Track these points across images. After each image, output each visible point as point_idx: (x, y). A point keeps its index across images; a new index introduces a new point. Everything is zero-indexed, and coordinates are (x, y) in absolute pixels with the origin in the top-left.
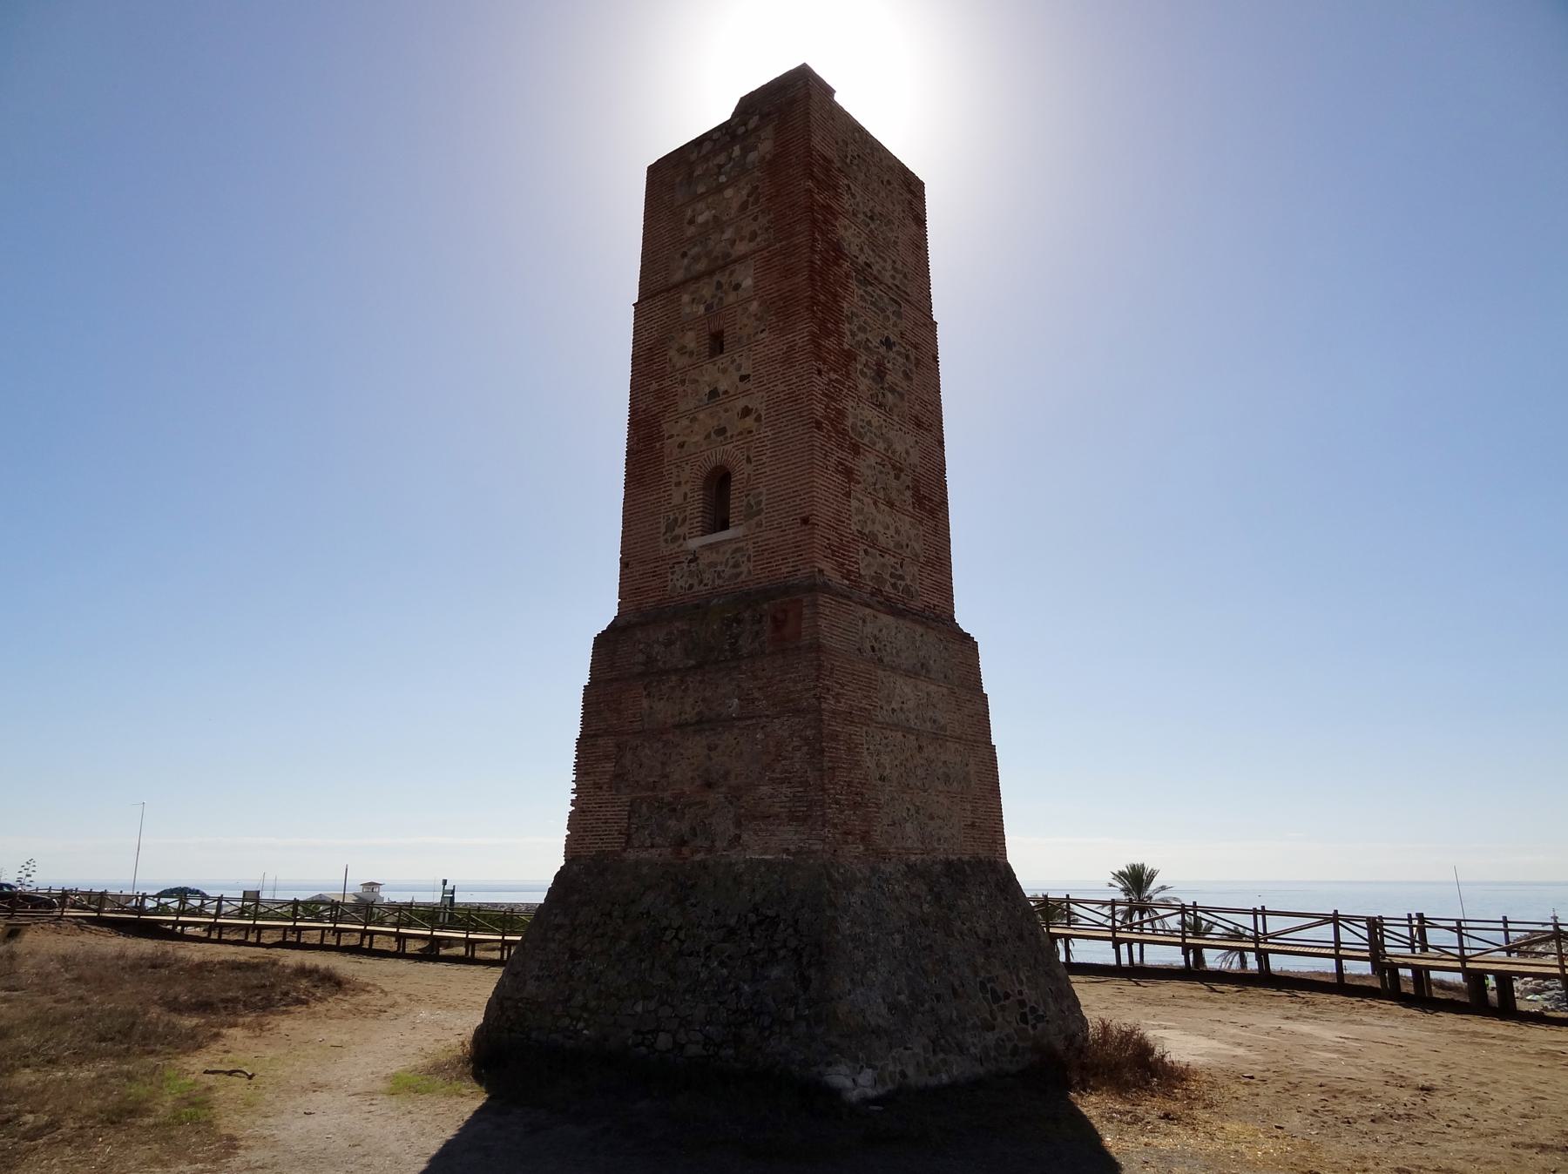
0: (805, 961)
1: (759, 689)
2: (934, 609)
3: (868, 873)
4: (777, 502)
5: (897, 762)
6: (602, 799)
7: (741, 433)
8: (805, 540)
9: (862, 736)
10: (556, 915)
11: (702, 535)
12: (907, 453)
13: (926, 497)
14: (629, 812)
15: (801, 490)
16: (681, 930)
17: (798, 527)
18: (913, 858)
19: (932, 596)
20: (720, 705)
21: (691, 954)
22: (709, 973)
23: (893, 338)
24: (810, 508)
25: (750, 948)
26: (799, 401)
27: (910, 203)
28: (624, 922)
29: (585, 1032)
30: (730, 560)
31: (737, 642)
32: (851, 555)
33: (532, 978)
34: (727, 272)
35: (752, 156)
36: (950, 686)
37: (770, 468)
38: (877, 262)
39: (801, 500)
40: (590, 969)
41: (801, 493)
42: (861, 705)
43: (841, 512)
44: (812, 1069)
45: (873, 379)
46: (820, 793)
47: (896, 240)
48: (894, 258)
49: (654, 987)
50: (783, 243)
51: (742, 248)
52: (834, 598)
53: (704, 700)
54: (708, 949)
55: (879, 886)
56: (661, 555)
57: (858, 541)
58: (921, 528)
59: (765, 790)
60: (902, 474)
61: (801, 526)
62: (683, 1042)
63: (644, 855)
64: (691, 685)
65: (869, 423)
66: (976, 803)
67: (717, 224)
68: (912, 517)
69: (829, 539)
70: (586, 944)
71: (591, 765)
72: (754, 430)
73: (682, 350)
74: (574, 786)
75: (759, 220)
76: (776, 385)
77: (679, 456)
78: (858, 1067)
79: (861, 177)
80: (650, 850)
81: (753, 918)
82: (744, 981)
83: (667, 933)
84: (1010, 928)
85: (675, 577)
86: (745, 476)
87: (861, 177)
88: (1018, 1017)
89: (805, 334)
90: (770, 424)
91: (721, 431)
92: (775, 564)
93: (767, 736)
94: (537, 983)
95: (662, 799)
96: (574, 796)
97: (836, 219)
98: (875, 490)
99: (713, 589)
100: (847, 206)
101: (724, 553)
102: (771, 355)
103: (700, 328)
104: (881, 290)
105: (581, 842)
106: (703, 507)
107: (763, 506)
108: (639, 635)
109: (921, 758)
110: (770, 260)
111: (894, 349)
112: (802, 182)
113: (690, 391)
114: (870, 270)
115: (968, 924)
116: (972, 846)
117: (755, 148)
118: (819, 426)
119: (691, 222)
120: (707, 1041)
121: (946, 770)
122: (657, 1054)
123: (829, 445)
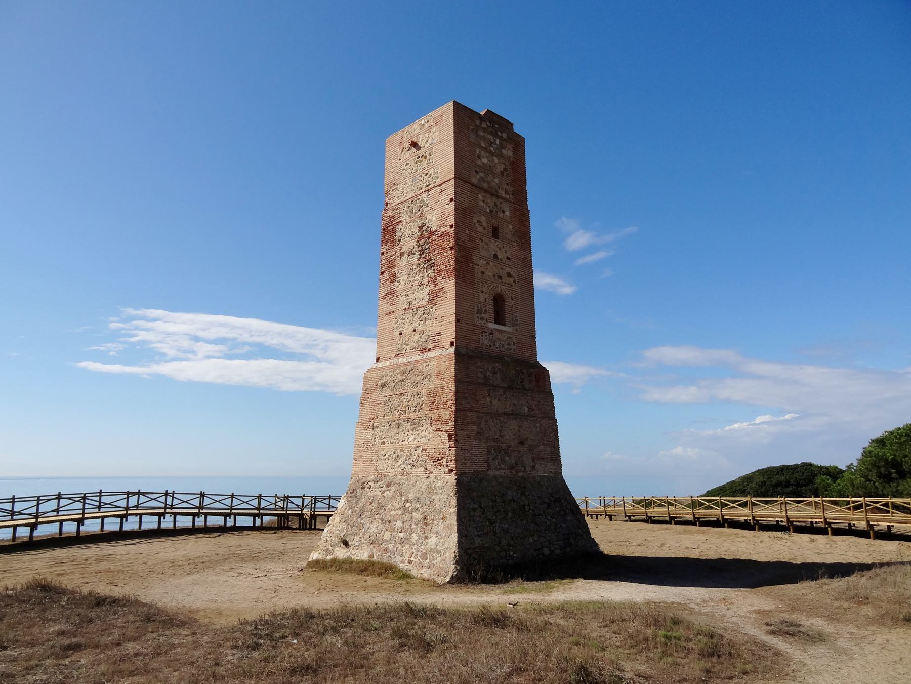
1: (536, 405)
7: (508, 284)
21: (539, 515)
29: (515, 555)
31: (523, 382)
33: (476, 536)
53: (514, 404)
59: (542, 448)
62: (553, 550)
63: (497, 473)
64: (508, 396)
71: (465, 425)
80: (500, 471)
93: (540, 425)
94: (480, 538)
95: (501, 447)
101: (504, 336)
108: (479, 364)
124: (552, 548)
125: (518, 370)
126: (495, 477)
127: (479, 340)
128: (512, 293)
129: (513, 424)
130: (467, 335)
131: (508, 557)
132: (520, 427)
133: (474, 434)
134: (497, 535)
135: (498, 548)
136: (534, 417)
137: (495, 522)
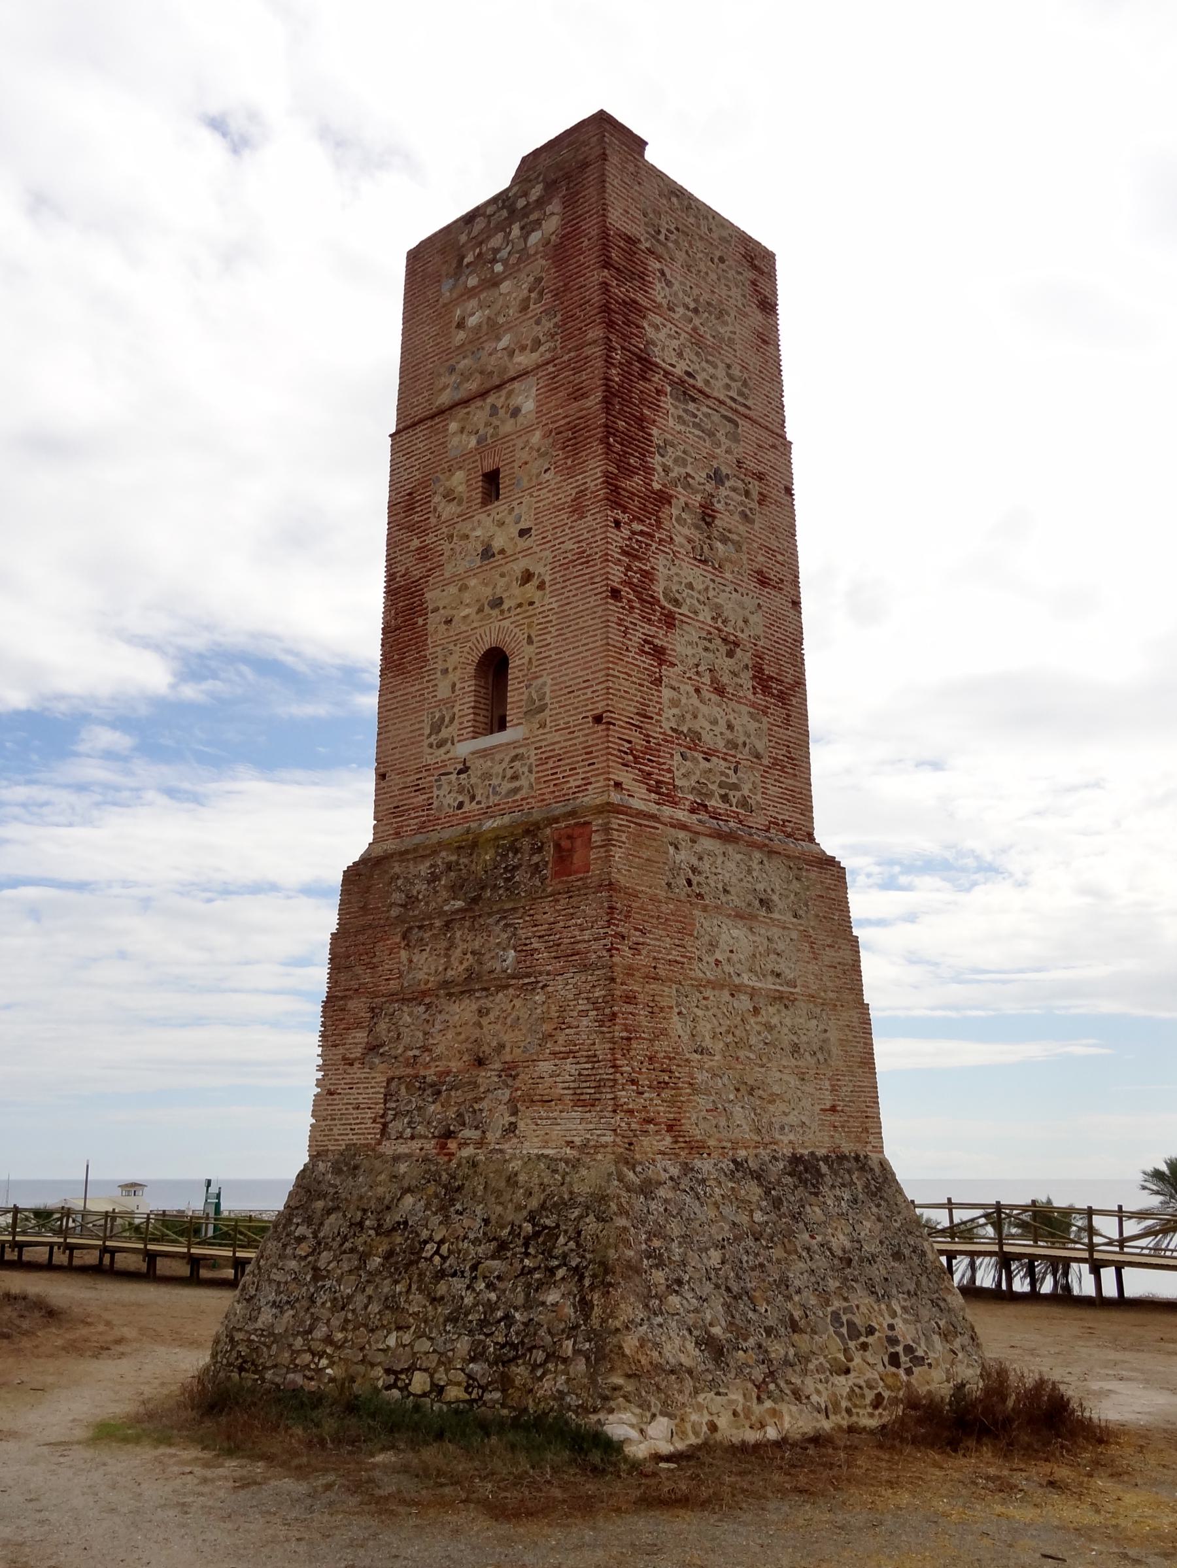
0: (587, 1283)
2: (783, 826)
3: (675, 1171)
4: (565, 695)
5: (723, 1029)
6: (353, 1078)
7: (520, 605)
8: (597, 745)
9: (671, 997)
10: (298, 1225)
11: (474, 738)
12: (746, 621)
13: (772, 678)
14: (385, 1095)
15: (594, 679)
16: (444, 1244)
17: (589, 728)
18: (742, 1153)
19: (781, 808)
20: (493, 958)
21: (454, 1275)
22: (475, 1298)
23: (725, 470)
24: (604, 703)
25: (524, 1267)
26: (591, 563)
27: (754, 283)
28: (377, 1234)
29: (329, 1371)
32: (662, 760)
33: (267, 1304)
34: (504, 392)
35: (535, 238)
36: (802, 928)
38: (704, 370)
39: (593, 692)
40: (335, 1292)
41: (594, 683)
42: (670, 957)
43: (648, 706)
44: (591, 1416)
45: (697, 527)
46: (611, 1070)
47: (733, 336)
48: (728, 361)
49: (411, 1315)
50: (572, 354)
51: (524, 360)
52: (634, 820)
54: (474, 1268)
55: (692, 1188)
57: (672, 742)
58: (765, 719)
60: (738, 650)
61: (593, 727)
62: (442, 1383)
63: (403, 1149)
65: (690, 586)
66: (839, 1080)
67: (493, 328)
68: (754, 707)
69: (630, 742)
70: (331, 1262)
73: (449, 496)
74: (321, 1062)
75: (543, 321)
76: (563, 542)
78: (648, 1415)
79: (680, 256)
81: (528, 1228)
82: (516, 1309)
83: (428, 1246)
84: (881, 1242)
85: (441, 793)
86: (526, 660)
87: (680, 256)
88: (886, 1359)
89: (599, 475)
90: (556, 593)
91: (497, 603)
92: (561, 776)
95: (425, 1077)
96: (320, 1075)
97: (644, 317)
98: (697, 673)
99: (488, 807)
100: (659, 299)
102: (557, 503)
103: (470, 467)
104: (708, 406)
105: (327, 1133)
106: (475, 701)
107: (547, 700)
109: (757, 1023)
110: (554, 378)
111: (727, 484)
112: (595, 272)
114: (691, 381)
115: (819, 1238)
116: (832, 1137)
117: (538, 223)
118: (615, 594)
119: (461, 325)
120: (471, 1382)
121: (795, 1038)
122: (411, 1397)
123: (629, 619)
124: (441, 1377)
126: (397, 1158)
127: (431, 801)
129: (462, 1011)
131: (310, 1370)
132: (481, 1012)
133: (357, 1052)
134: (312, 1310)
135: (299, 1342)
136: (528, 975)
137: (324, 1278)
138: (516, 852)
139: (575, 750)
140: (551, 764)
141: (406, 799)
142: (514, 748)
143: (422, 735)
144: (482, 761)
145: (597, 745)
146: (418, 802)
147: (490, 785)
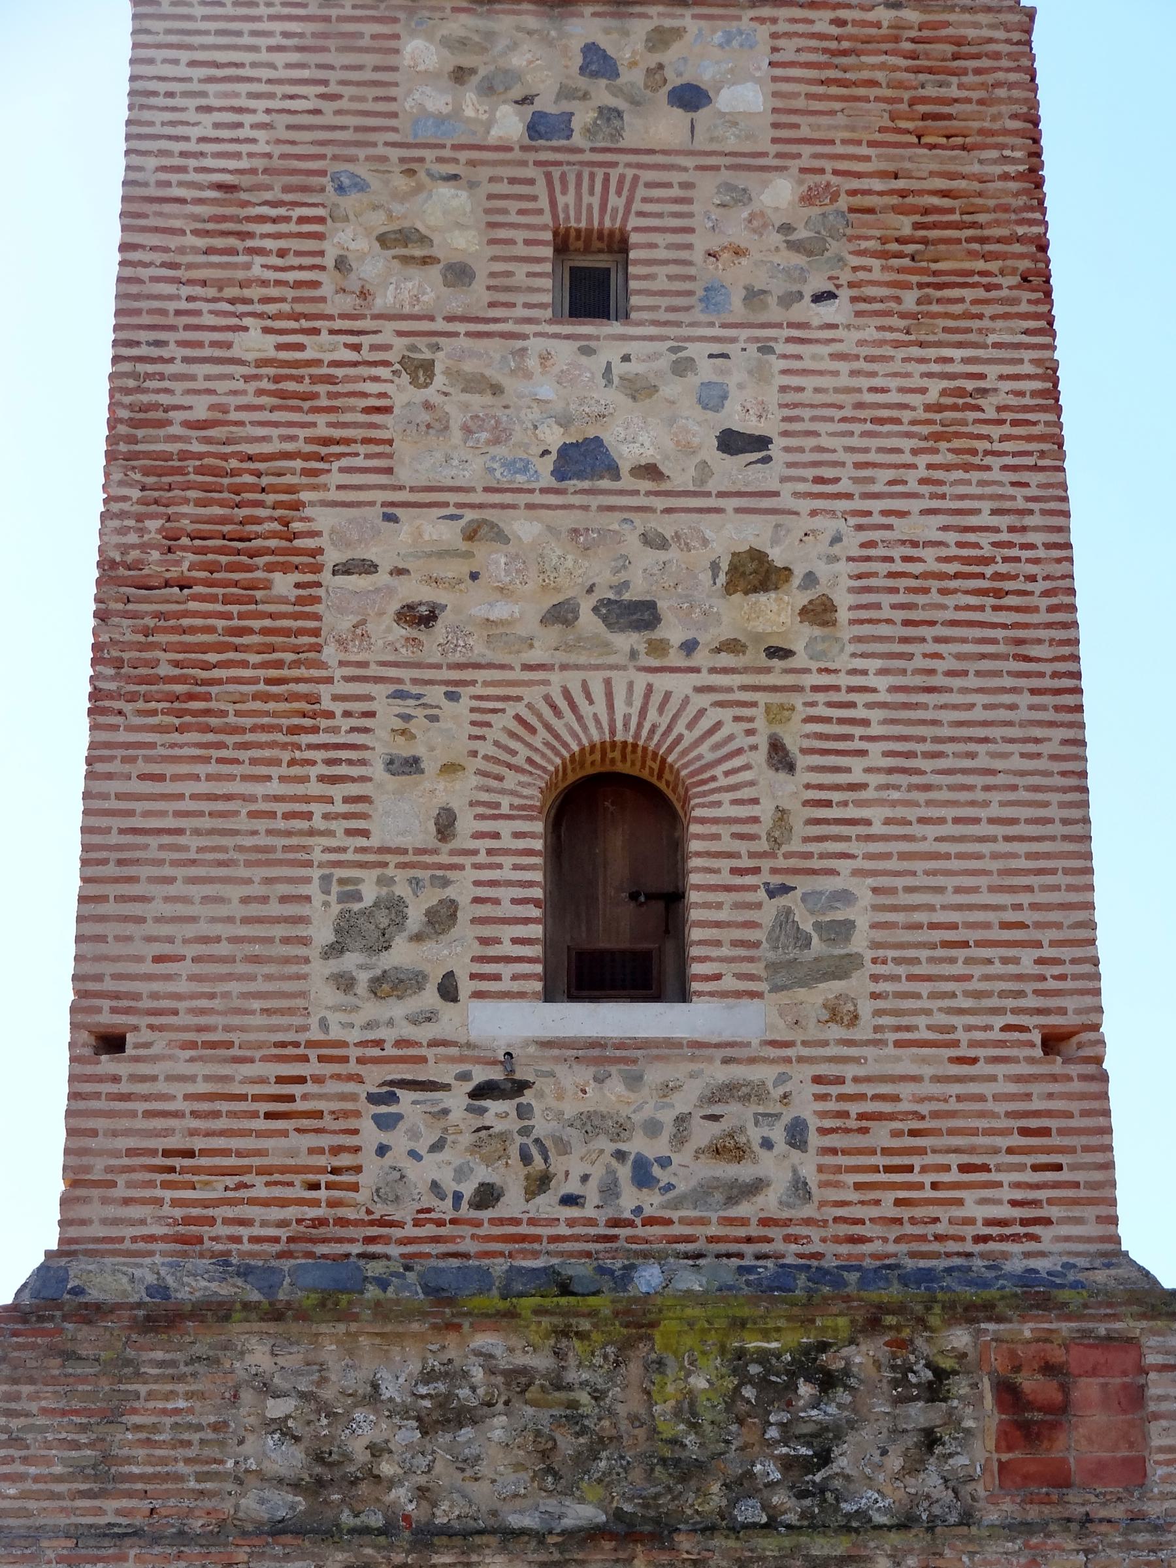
4: (933, 946)
7: (732, 646)
8: (1069, 1115)
17: (1031, 1060)
30: (697, 1123)
31: (824, 1458)
37: (889, 812)
39: (1040, 961)
56: (316, 1034)
72: (798, 646)
77: (405, 654)
85: (398, 1140)
86: (765, 811)
101: (667, 1089)
107: (859, 943)
108: (259, 1357)
110: (844, 53)
113: (457, 418)
125: (763, 1357)
127: (345, 1160)
128: (776, 714)
130: (198, 1144)
138: (828, 1382)
139: (982, 1114)
140: (881, 1136)
141: (222, 1133)
142: (726, 1061)
143: (305, 941)
144: (584, 1074)
145: (1069, 1115)
146: (293, 1153)
147: (620, 1155)
